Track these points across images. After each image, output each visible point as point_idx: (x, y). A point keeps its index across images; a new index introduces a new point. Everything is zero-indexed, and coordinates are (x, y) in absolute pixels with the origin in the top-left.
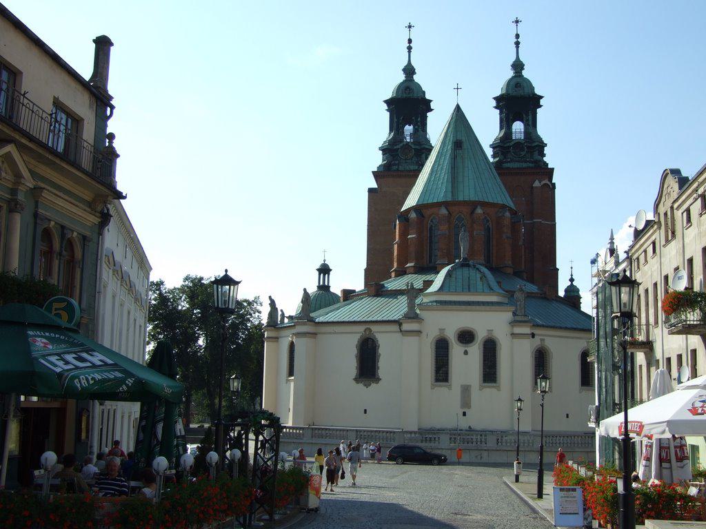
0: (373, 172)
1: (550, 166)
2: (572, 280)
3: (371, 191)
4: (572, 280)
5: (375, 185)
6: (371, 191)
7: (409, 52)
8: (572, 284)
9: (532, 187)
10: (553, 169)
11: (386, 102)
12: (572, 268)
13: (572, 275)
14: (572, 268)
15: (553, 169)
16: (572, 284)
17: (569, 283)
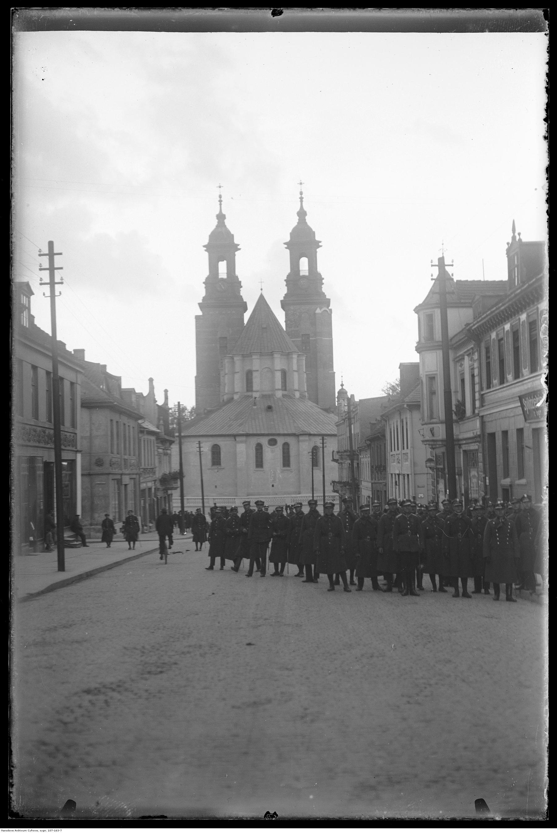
0: (199, 304)
1: (327, 297)
2: (342, 385)
3: (197, 318)
4: (342, 385)
5: (200, 313)
6: (197, 318)
7: (221, 204)
8: (342, 388)
9: (315, 313)
10: (329, 300)
11: (204, 246)
12: (342, 377)
13: (342, 382)
14: (342, 377)
15: (329, 300)
16: (342, 388)
17: (341, 387)
